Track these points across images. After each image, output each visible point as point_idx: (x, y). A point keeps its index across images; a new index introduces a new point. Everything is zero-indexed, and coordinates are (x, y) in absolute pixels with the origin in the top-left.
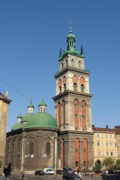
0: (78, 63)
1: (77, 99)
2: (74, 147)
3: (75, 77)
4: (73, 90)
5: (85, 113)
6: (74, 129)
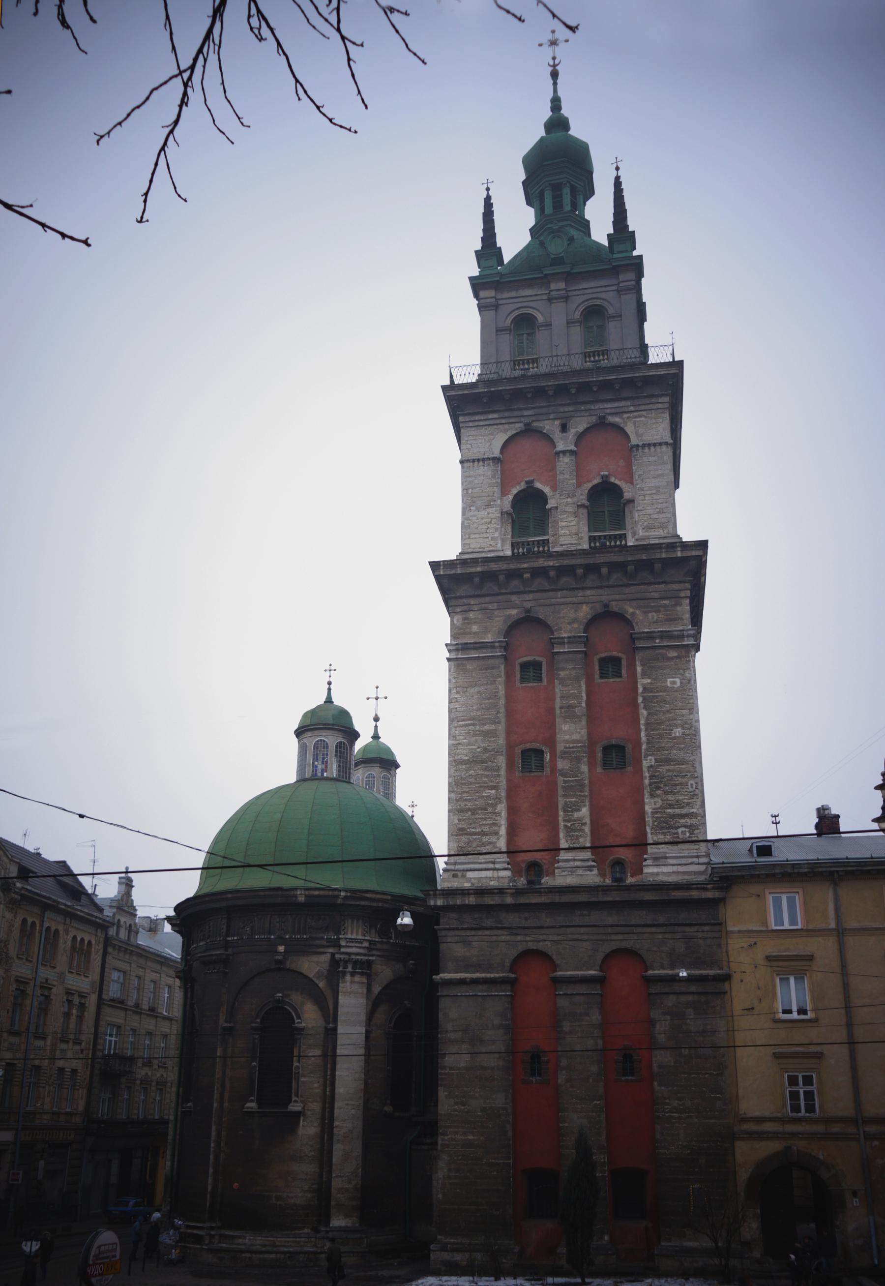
3: (527, 445)
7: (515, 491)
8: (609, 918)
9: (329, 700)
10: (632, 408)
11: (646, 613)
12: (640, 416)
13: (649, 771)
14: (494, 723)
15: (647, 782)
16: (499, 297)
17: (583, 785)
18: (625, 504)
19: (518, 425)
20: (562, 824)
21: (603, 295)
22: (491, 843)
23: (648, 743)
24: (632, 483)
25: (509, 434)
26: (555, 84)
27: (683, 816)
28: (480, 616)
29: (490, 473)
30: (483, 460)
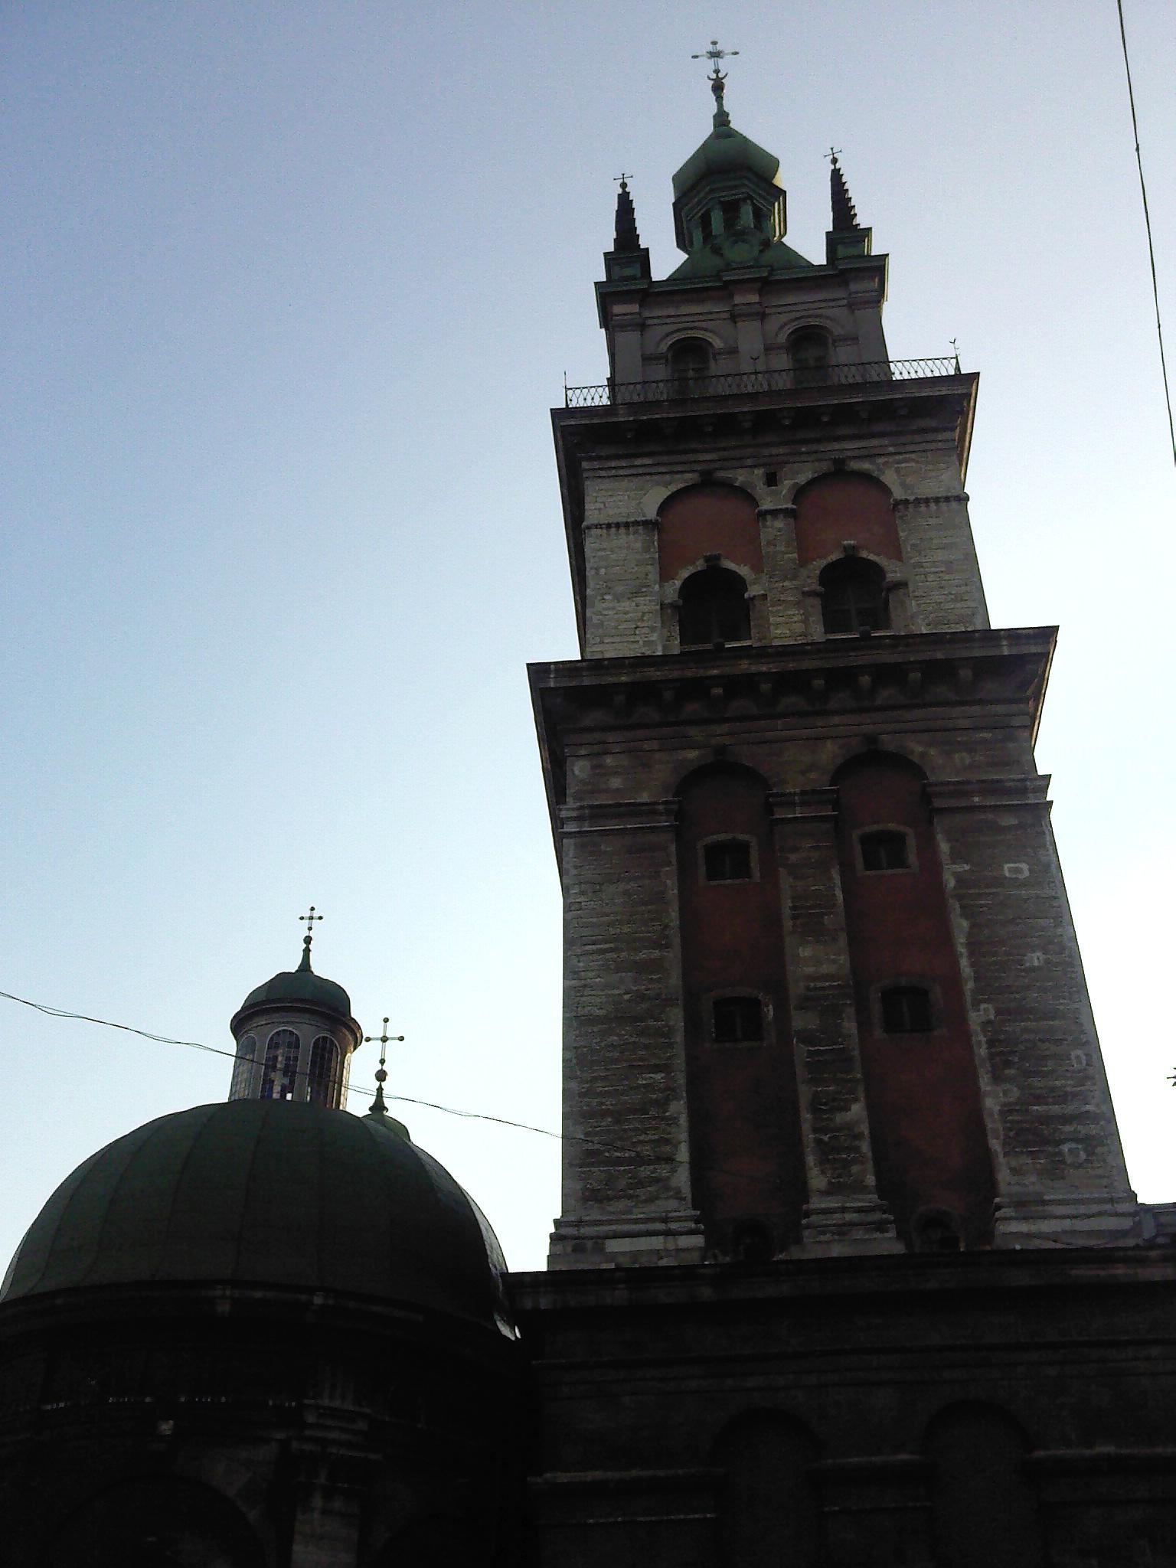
7: (685, 574)
10: (891, 449)
12: (905, 461)
13: (984, 1031)
14: (657, 945)
15: (983, 1051)
16: (647, 314)
19: (690, 475)
20: (809, 1137)
22: (658, 1180)
23: (977, 979)
24: (900, 558)
25: (673, 488)
26: (719, 98)
27: (1067, 1119)
28: (626, 763)
29: (639, 545)
30: (627, 525)
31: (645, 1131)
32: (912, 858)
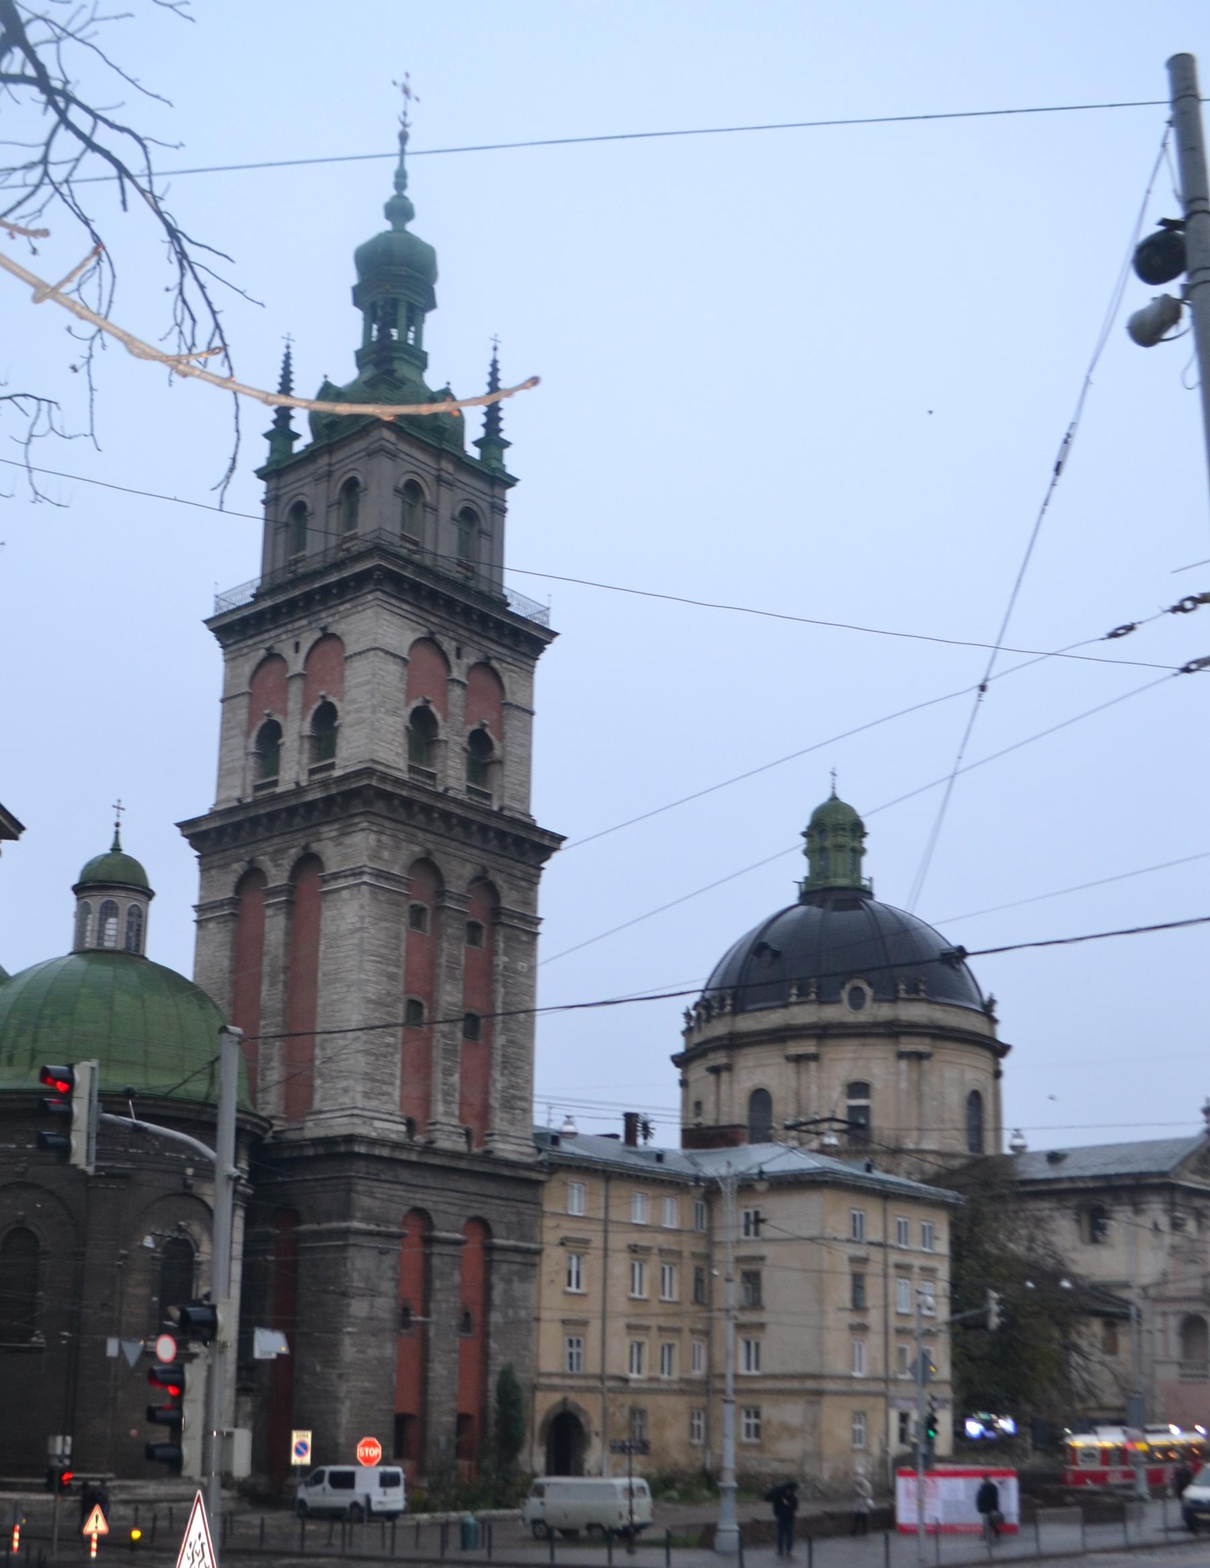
0: (455, 530)
1: (438, 859)
2: (387, 1286)
3: (427, 657)
4: (405, 776)
5: (490, 994)
6: (395, 1130)
8: (472, 1186)
9: (116, 848)
10: (510, 660)
11: (510, 889)
14: (396, 966)
15: (499, 1059)
17: (456, 1051)
18: (493, 762)
19: (424, 630)
21: (478, 501)
25: (418, 635)
29: (398, 675)
30: (395, 656)
31: (385, 1067)
32: (484, 942)
